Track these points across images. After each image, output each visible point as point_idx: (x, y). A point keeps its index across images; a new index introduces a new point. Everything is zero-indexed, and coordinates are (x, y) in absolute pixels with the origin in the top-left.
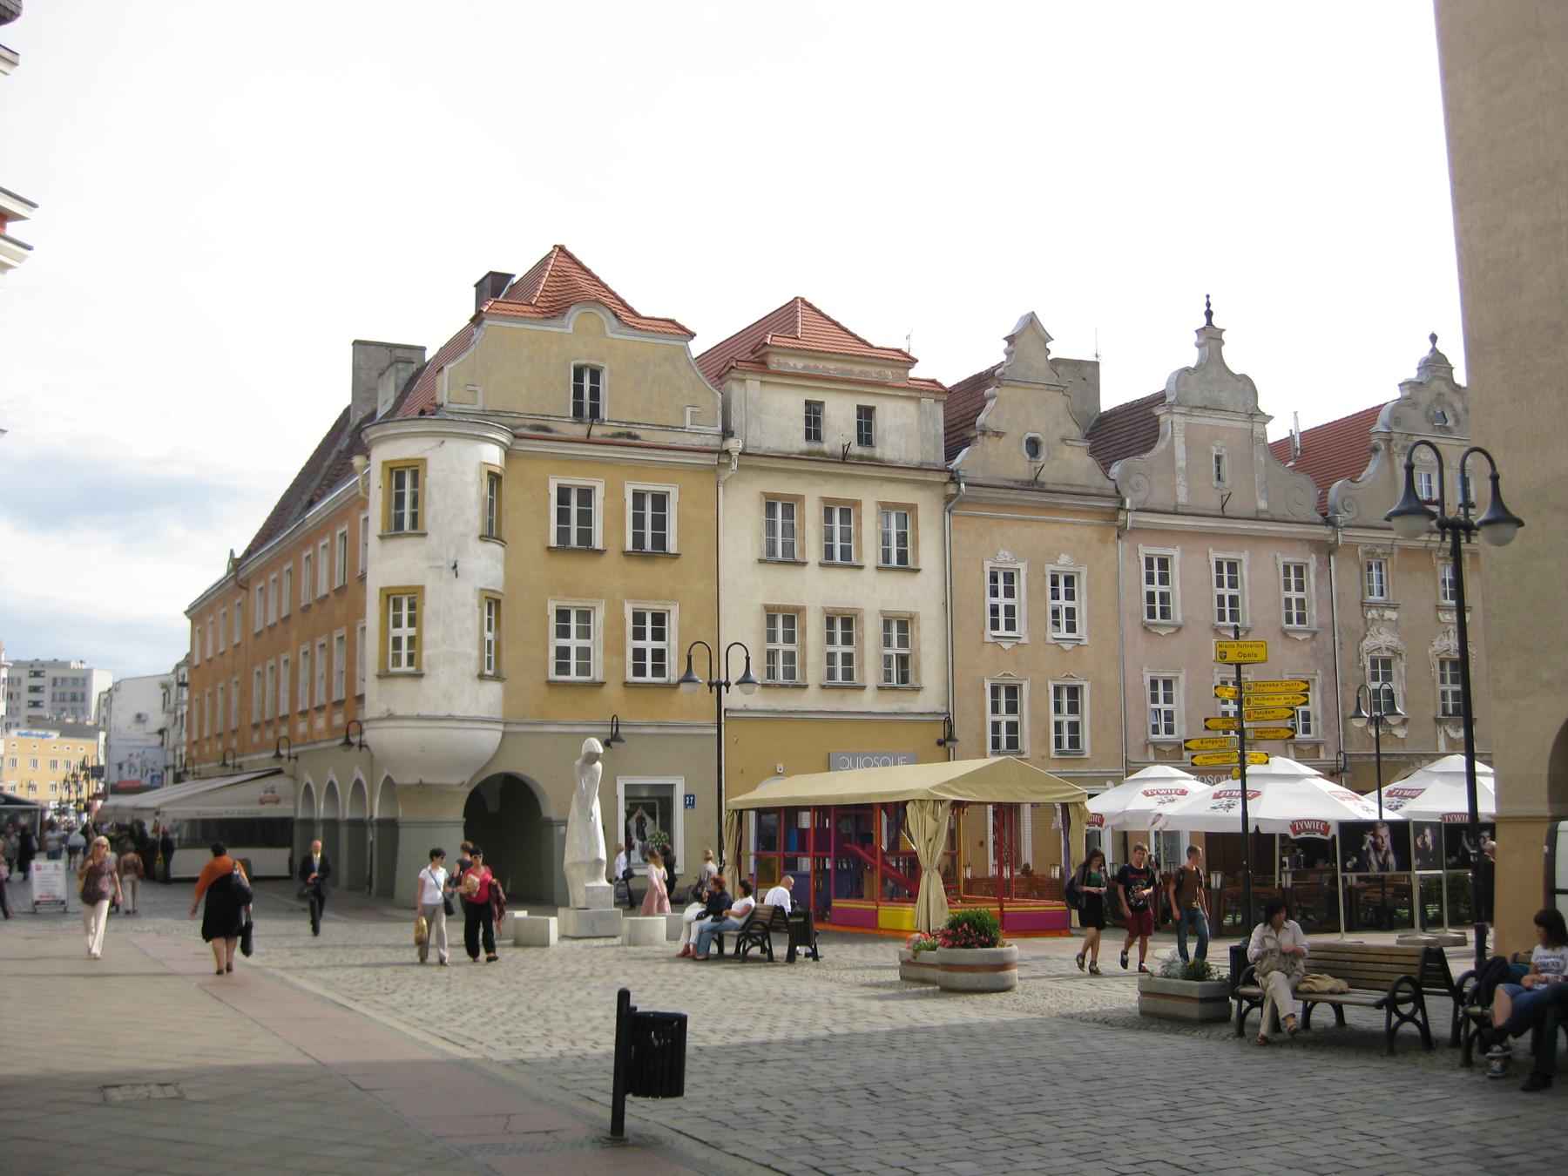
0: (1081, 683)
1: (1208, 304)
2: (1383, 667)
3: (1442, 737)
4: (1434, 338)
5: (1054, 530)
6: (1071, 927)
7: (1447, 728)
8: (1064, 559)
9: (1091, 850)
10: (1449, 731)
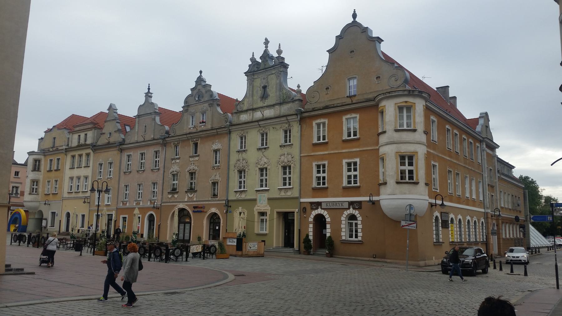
0: (110, 188)
1: (149, 86)
2: (175, 176)
3: (187, 196)
4: (201, 72)
5: (110, 153)
6: (212, 255)
7: (188, 194)
8: (110, 159)
9: (117, 228)
10: (189, 195)
